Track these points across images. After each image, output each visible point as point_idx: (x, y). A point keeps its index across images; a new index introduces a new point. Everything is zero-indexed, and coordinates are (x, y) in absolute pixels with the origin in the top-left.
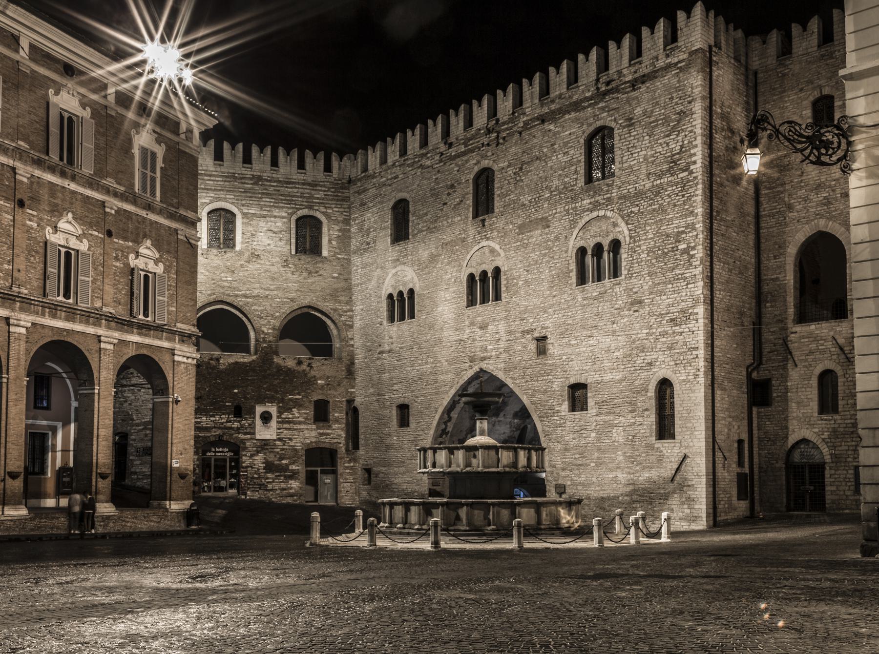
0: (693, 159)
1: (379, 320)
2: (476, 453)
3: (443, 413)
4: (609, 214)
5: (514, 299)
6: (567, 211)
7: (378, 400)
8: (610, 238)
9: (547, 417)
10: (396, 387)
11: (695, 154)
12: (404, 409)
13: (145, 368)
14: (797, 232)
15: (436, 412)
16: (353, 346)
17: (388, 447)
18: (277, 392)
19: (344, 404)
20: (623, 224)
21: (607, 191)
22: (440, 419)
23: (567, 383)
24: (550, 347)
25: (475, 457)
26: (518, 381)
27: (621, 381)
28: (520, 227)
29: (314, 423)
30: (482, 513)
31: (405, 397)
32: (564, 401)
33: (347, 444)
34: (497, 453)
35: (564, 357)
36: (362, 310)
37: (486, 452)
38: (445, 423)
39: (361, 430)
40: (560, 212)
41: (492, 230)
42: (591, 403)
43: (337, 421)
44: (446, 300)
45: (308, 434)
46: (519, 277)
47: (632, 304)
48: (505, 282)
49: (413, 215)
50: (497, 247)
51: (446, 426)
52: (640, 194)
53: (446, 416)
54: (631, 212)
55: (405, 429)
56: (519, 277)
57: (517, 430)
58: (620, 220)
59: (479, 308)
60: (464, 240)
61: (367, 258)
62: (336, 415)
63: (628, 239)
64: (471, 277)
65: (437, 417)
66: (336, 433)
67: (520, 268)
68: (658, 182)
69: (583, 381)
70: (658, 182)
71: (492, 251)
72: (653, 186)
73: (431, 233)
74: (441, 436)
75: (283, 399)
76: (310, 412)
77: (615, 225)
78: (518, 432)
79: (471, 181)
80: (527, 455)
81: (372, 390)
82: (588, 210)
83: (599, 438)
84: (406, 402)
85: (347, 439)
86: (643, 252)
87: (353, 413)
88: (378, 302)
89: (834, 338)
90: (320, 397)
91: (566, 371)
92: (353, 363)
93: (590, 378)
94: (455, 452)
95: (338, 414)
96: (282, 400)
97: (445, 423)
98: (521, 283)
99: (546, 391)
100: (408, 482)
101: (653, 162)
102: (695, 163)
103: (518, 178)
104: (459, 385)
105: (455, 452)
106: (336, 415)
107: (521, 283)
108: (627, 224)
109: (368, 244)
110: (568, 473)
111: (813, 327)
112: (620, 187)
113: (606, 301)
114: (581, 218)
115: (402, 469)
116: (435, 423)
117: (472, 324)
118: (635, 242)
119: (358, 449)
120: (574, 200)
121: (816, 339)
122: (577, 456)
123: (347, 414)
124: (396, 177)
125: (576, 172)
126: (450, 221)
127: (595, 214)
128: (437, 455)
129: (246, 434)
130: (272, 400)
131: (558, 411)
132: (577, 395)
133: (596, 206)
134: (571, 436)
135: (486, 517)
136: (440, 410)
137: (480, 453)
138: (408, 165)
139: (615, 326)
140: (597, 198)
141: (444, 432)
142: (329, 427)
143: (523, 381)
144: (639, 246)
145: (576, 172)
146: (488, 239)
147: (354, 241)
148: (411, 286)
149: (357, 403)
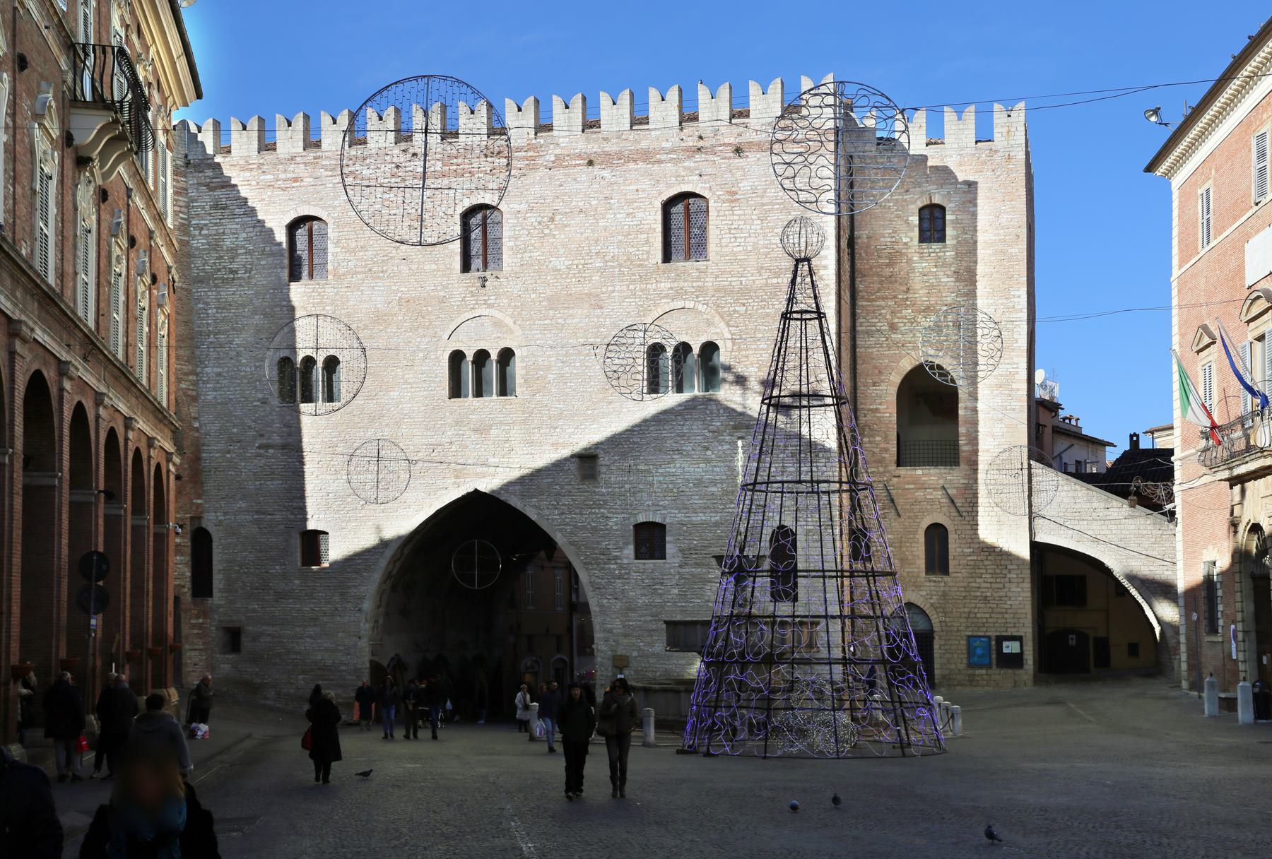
0: (824, 263)
1: (260, 396)
4: (701, 307)
5: (538, 397)
6: (634, 292)
8: (704, 339)
11: (826, 257)
14: (901, 357)
16: (197, 430)
17: (281, 596)
20: (722, 325)
21: (698, 277)
23: (633, 521)
24: (604, 469)
27: (716, 524)
28: (549, 299)
32: (627, 544)
36: (219, 374)
40: (620, 292)
41: (498, 295)
42: (670, 549)
44: (406, 383)
46: (549, 368)
47: (735, 428)
48: (524, 372)
49: (337, 244)
50: (509, 321)
52: (746, 291)
54: (735, 311)
56: (549, 368)
58: (717, 318)
59: (470, 402)
60: (442, 300)
61: (228, 293)
63: (729, 344)
64: (457, 358)
67: (550, 356)
68: (775, 281)
69: (658, 520)
70: (775, 281)
71: (498, 324)
72: (767, 285)
73: (374, 278)
77: (709, 323)
79: (457, 219)
82: (667, 296)
83: (682, 596)
86: (752, 364)
88: (256, 367)
89: (944, 488)
92: (198, 459)
93: (669, 517)
98: (551, 377)
99: (595, 530)
101: (766, 254)
102: (825, 267)
103: (547, 231)
107: (551, 377)
108: (728, 326)
109: (232, 271)
111: (919, 472)
112: (717, 277)
113: (697, 420)
114: (656, 305)
115: (311, 630)
117: (458, 423)
118: (739, 350)
119: (211, 595)
120: (644, 278)
121: (923, 487)
124: (296, 180)
125: (647, 242)
126: (414, 267)
127: (679, 304)
131: (616, 558)
132: (650, 539)
133: (679, 293)
134: (639, 592)
138: (324, 167)
139: (709, 453)
140: (682, 284)
144: (747, 356)
145: (647, 242)
146: (490, 306)
147: (199, 262)
148: (331, 352)
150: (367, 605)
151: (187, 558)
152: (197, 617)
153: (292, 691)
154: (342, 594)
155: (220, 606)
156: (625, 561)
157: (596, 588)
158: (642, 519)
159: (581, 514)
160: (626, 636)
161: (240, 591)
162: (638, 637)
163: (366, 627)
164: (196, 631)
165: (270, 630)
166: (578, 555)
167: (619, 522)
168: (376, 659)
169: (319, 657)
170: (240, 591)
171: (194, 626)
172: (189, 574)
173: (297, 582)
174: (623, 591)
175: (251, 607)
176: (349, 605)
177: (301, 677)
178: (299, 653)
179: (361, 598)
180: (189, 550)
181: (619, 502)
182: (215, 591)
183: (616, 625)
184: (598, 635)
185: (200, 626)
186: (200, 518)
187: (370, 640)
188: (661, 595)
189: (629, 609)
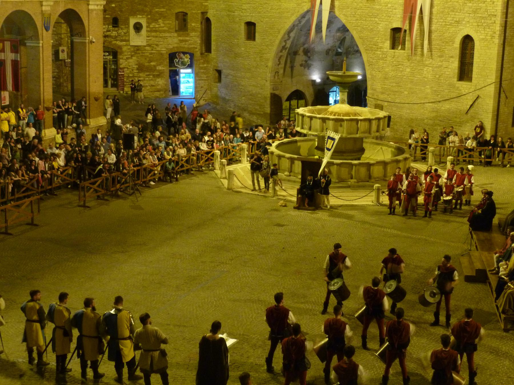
2: (343, 123)
3: (285, 34)
7: (228, 16)
9: (372, 50)
10: (245, 7)
12: (251, 26)
13: (71, 18)
15: (279, 32)
17: (237, 55)
18: (146, 6)
19: (200, 15)
22: (283, 38)
25: (341, 126)
26: (349, 19)
29: (176, 31)
30: (347, 170)
31: (252, 16)
32: (386, 40)
33: (201, 49)
34: (357, 124)
35: (389, 5)
37: (350, 122)
38: (285, 41)
39: (213, 38)
43: (194, 30)
45: (172, 41)
51: (286, 43)
53: (286, 36)
55: (251, 42)
57: (338, 40)
62: (193, 24)
65: (280, 37)
66: (194, 40)
74: (281, 51)
75: (151, 12)
76: (173, 23)
78: (339, 42)
80: (377, 124)
81: (223, 6)
84: (253, 21)
85: (201, 44)
87: (208, 21)
90: (181, 10)
91: (390, 17)
94: (327, 121)
95: (195, 24)
96: (150, 13)
97: (285, 41)
100: (254, 86)
104: (299, 14)
105: (327, 121)
106: (193, 24)
110: (386, 96)
116: (277, 42)
122: (394, 84)
123: (201, 23)
128: (312, 122)
129: (125, 41)
130: (142, 12)
131: (381, 48)
135: (350, 173)
136: (282, 32)
137: (345, 124)
141: (284, 48)
142: (188, 35)
143: (354, 19)
149: (210, 15)
150: (270, 64)
151: (199, 34)
152: (204, 63)
153: (240, 105)
154: (261, 57)
155: (214, 58)
156: (385, 50)
157: (370, 65)
158: (395, 26)
159: (365, 20)
160: (382, 93)
161: (222, 52)
162: (388, 95)
163: (269, 75)
164: (202, 71)
165: (232, 72)
166: (363, 44)
167: (384, 28)
168: (277, 92)
169: (250, 89)
170: (222, 52)
171: (201, 68)
172: (199, 42)
173: (243, 49)
174: (383, 68)
175: (225, 60)
176: (263, 63)
177: (243, 98)
178: (243, 86)
179: (268, 60)
180: (199, 30)
181: (385, 15)
182: (212, 50)
183: (378, 87)
184: (369, 92)
185: (205, 68)
186: (207, 12)
187: (271, 82)
188: (402, 71)
189: (385, 78)
